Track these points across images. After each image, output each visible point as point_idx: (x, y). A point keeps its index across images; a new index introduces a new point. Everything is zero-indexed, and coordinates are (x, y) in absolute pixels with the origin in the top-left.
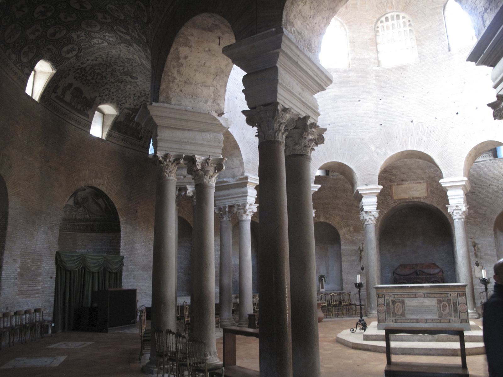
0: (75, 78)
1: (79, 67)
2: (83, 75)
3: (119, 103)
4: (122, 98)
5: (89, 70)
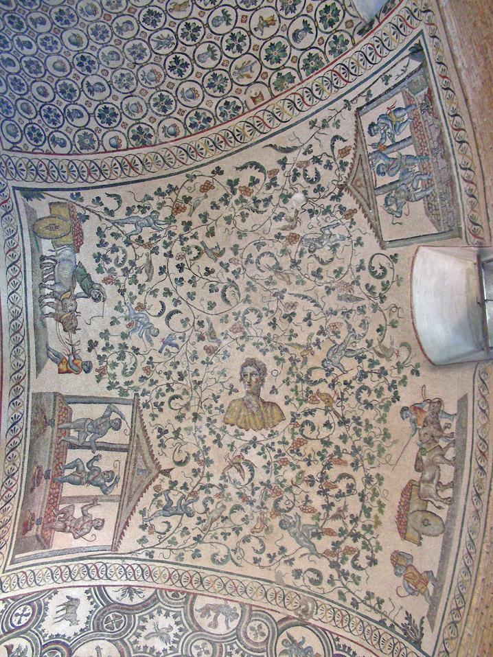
0: (373, 562)
1: (336, 577)
2: (356, 537)
3: (378, 290)
4: (358, 299)
5: (330, 532)
